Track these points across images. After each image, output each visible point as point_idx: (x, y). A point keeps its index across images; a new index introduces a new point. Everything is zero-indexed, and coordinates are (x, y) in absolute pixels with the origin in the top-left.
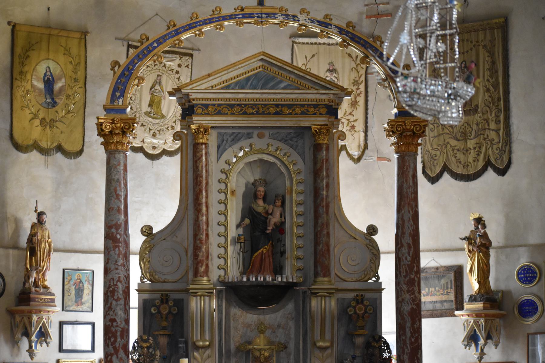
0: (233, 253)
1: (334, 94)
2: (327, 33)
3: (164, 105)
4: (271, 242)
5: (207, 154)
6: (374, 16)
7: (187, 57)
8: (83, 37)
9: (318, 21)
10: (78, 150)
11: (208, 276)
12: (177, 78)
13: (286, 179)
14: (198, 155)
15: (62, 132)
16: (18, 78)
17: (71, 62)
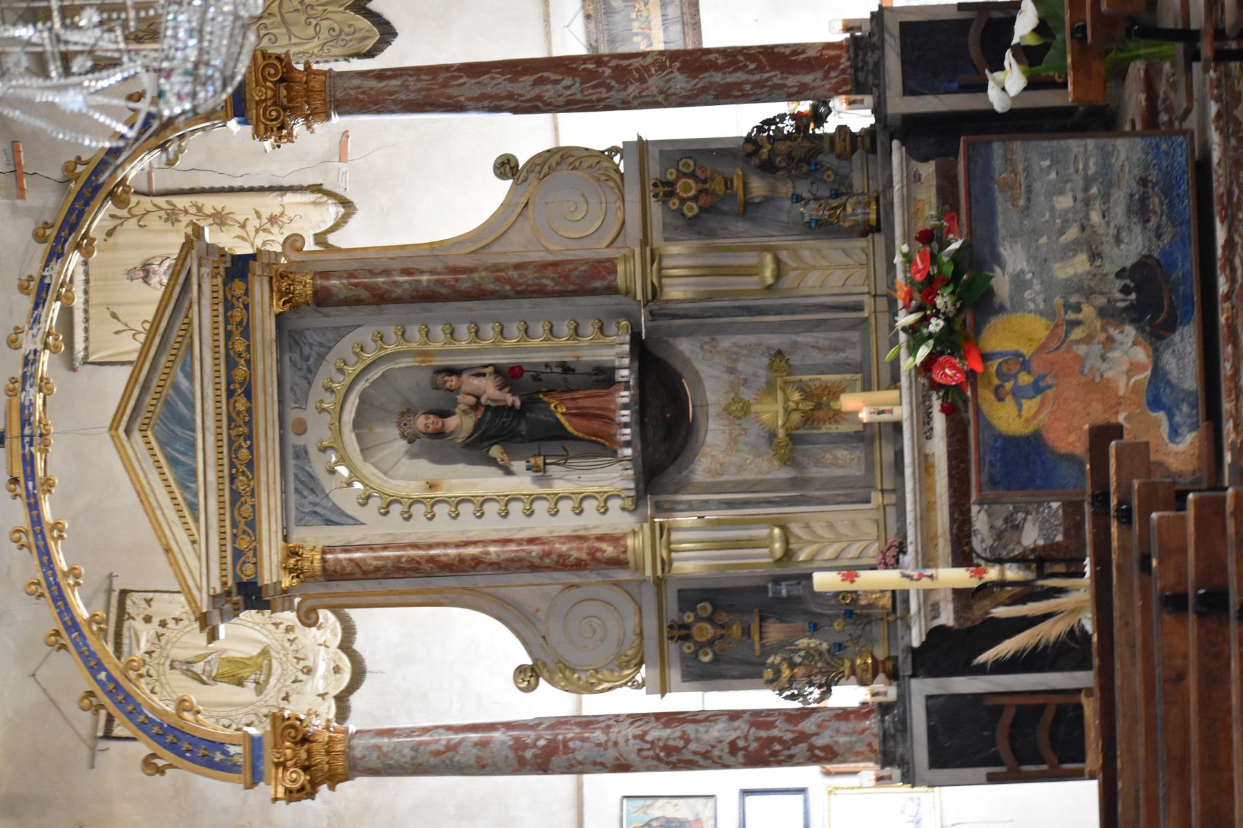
0: (569, 480)
1: (200, 266)
2: (62, 286)
3: (242, 652)
4: (541, 396)
5: (346, 549)
6: (19, 180)
7: (128, 602)
9: (36, 307)
11: (624, 537)
12: (177, 623)
13: (397, 366)
14: (349, 570)
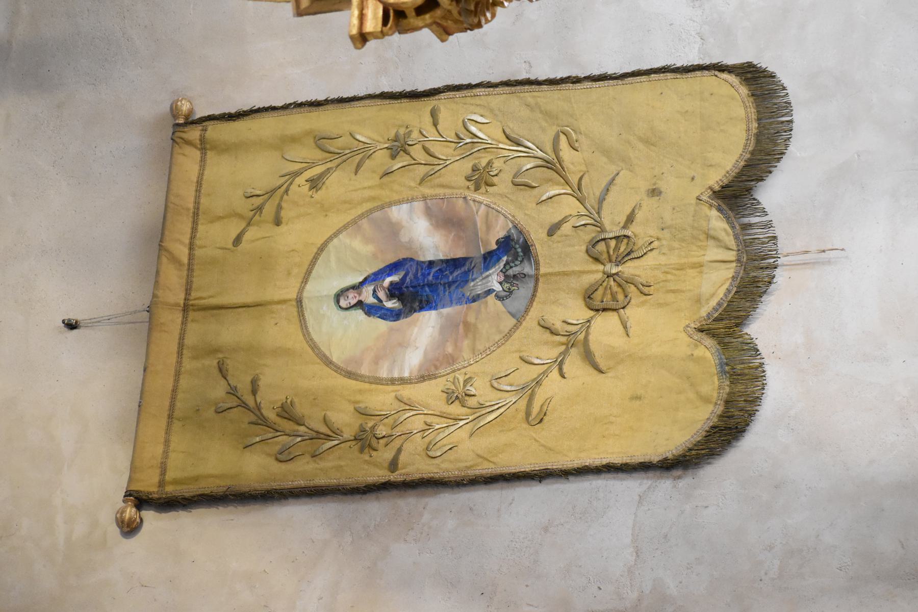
8: (194, 134)
10: (744, 90)
15: (654, 192)
16: (388, 455)
17: (315, 183)
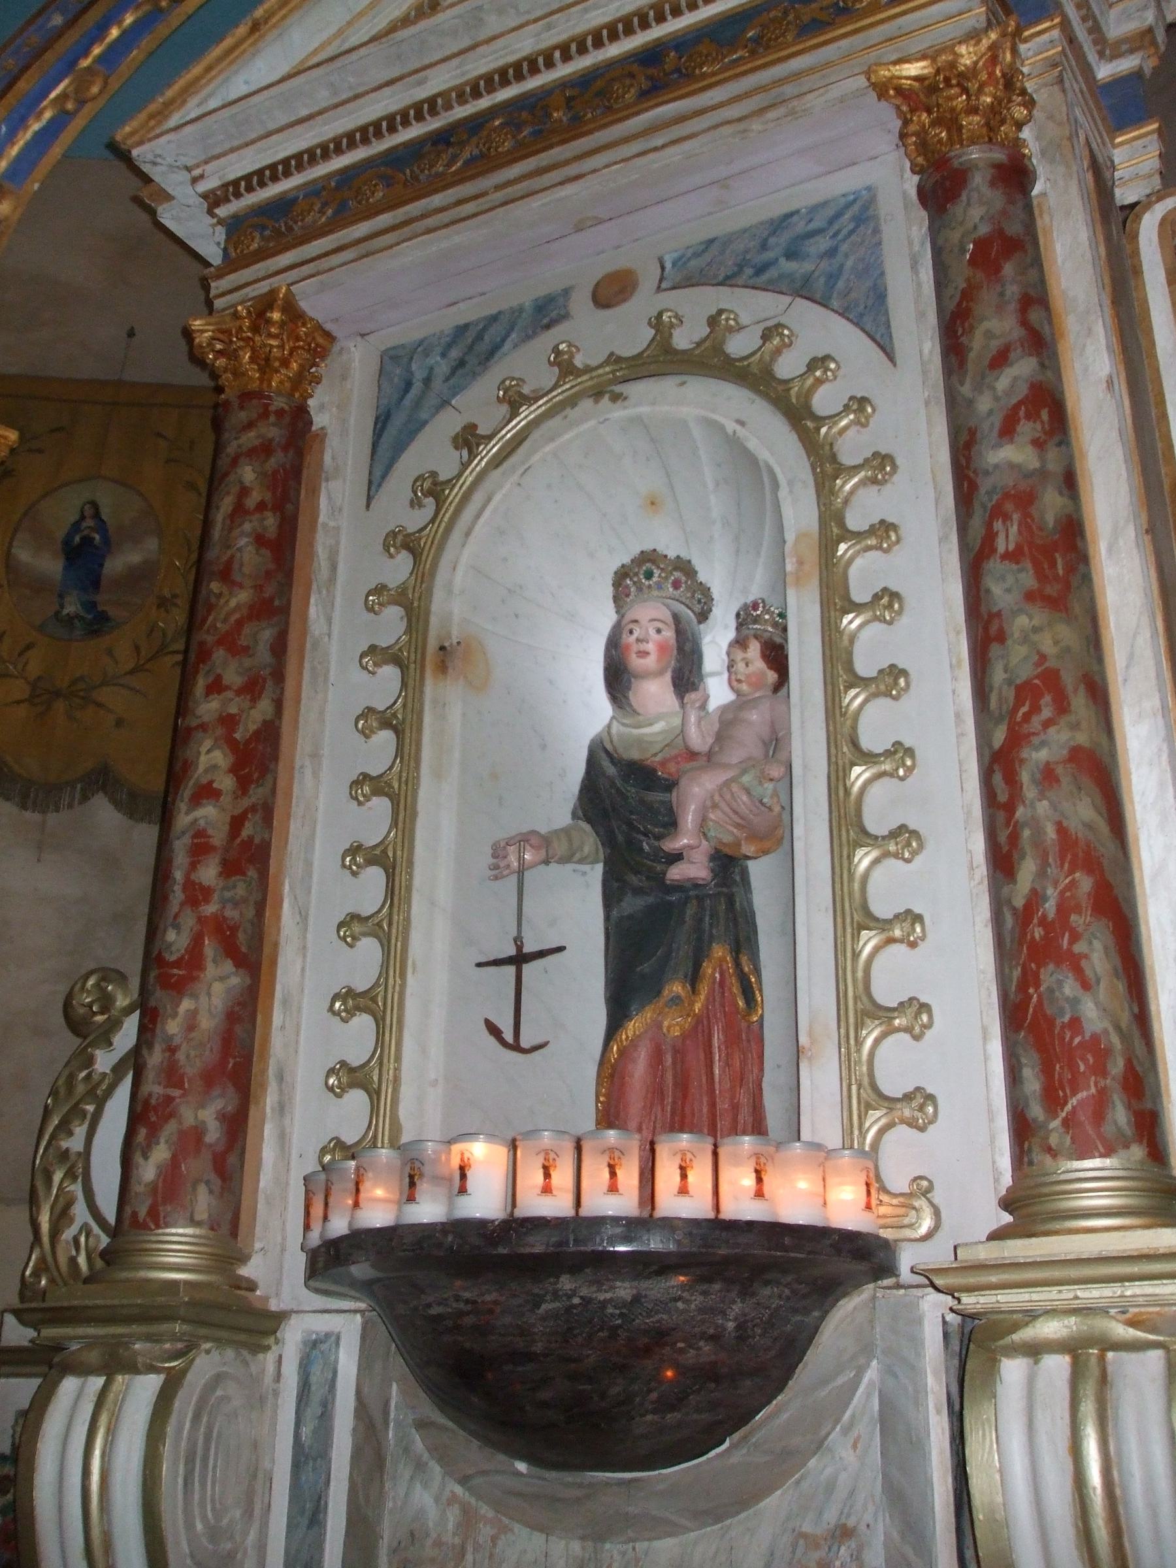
15: (119, 723)
